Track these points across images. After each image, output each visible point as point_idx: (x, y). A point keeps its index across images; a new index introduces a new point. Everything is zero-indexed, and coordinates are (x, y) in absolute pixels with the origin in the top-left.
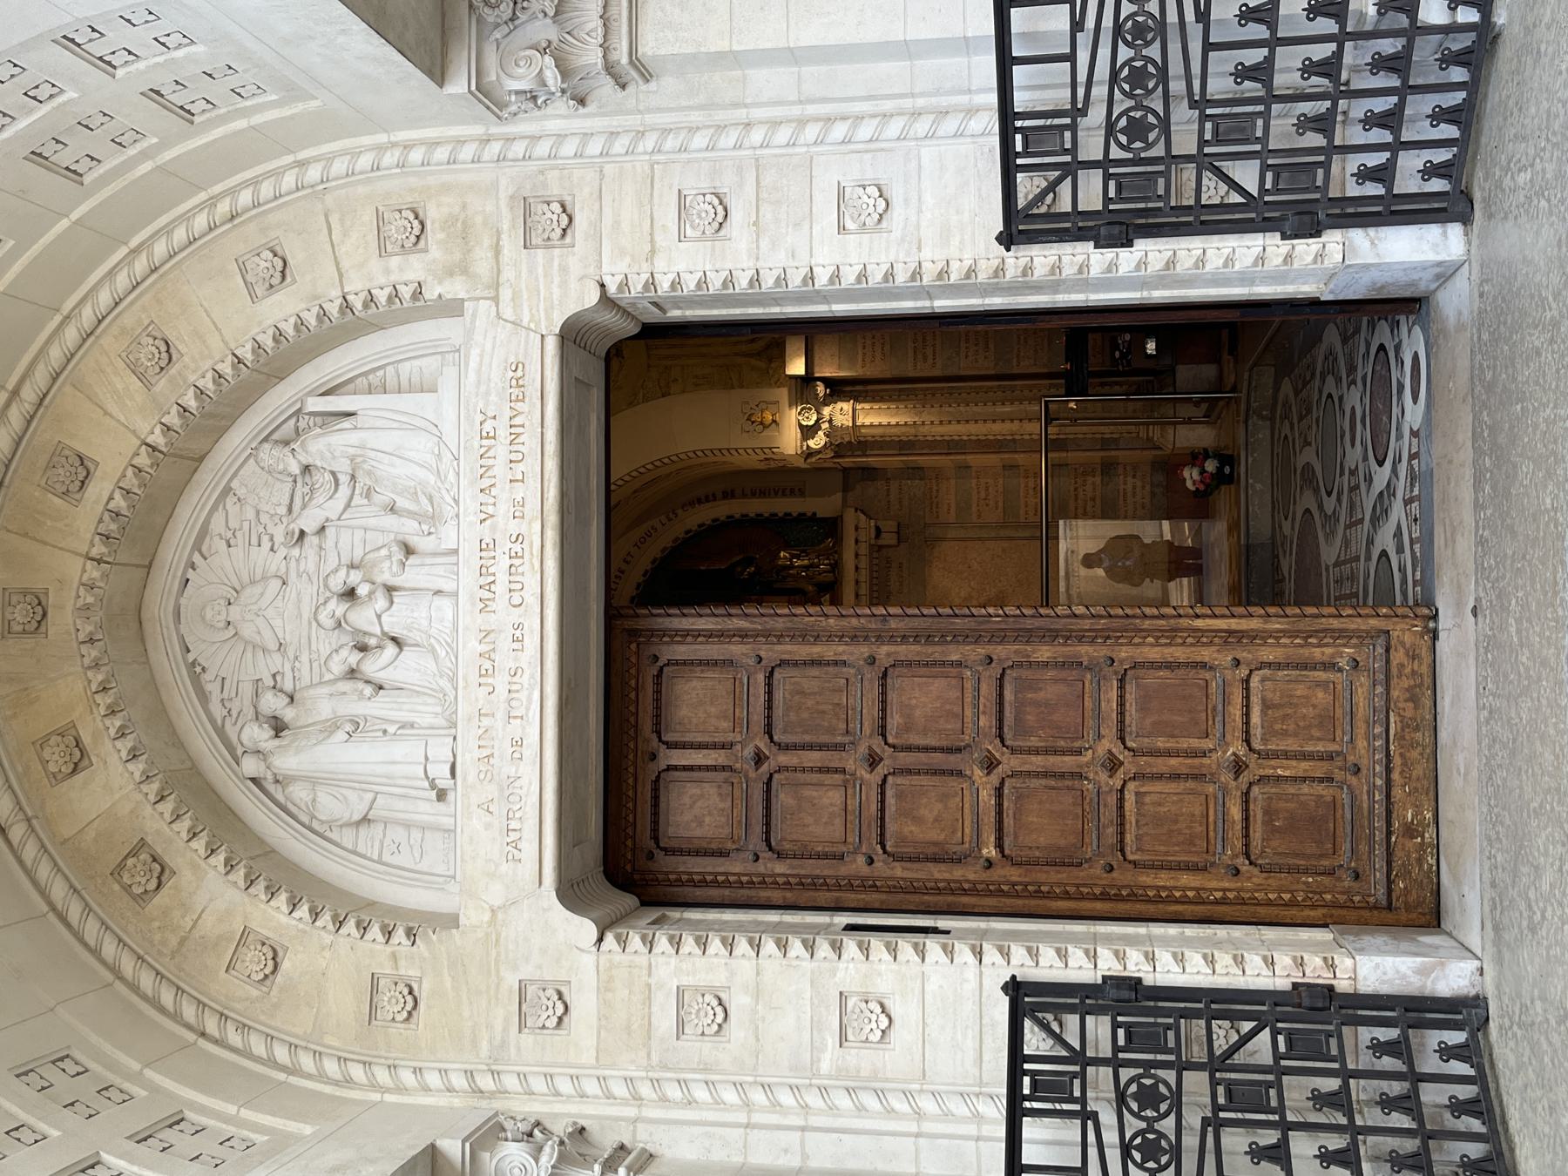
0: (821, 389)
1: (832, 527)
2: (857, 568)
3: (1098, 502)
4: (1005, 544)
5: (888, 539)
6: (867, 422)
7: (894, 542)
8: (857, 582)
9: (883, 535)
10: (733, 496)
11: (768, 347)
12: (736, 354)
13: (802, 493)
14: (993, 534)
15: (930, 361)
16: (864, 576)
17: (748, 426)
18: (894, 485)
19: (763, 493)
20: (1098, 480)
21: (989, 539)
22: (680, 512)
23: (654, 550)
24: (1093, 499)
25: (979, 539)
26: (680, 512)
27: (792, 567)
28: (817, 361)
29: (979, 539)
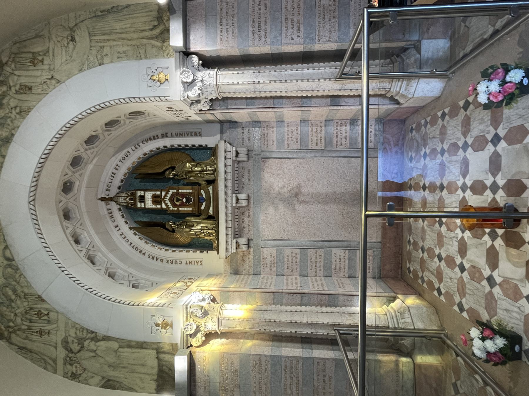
0: (195, 58)
1: (213, 151)
2: (226, 172)
3: (348, 139)
4: (301, 160)
5: (242, 157)
6: (225, 82)
7: (245, 159)
8: (226, 179)
9: (240, 155)
10: (167, 137)
11: (162, 33)
12: (143, 38)
13: (200, 135)
14: (295, 156)
15: (263, 39)
16: (229, 176)
17: (151, 83)
18: (246, 130)
19: (181, 135)
20: (348, 127)
21: (293, 158)
22: (141, 144)
23: (129, 163)
24: (346, 138)
25: (288, 158)
26: (141, 144)
27: (192, 171)
28: (192, 38)
29: (288, 158)
